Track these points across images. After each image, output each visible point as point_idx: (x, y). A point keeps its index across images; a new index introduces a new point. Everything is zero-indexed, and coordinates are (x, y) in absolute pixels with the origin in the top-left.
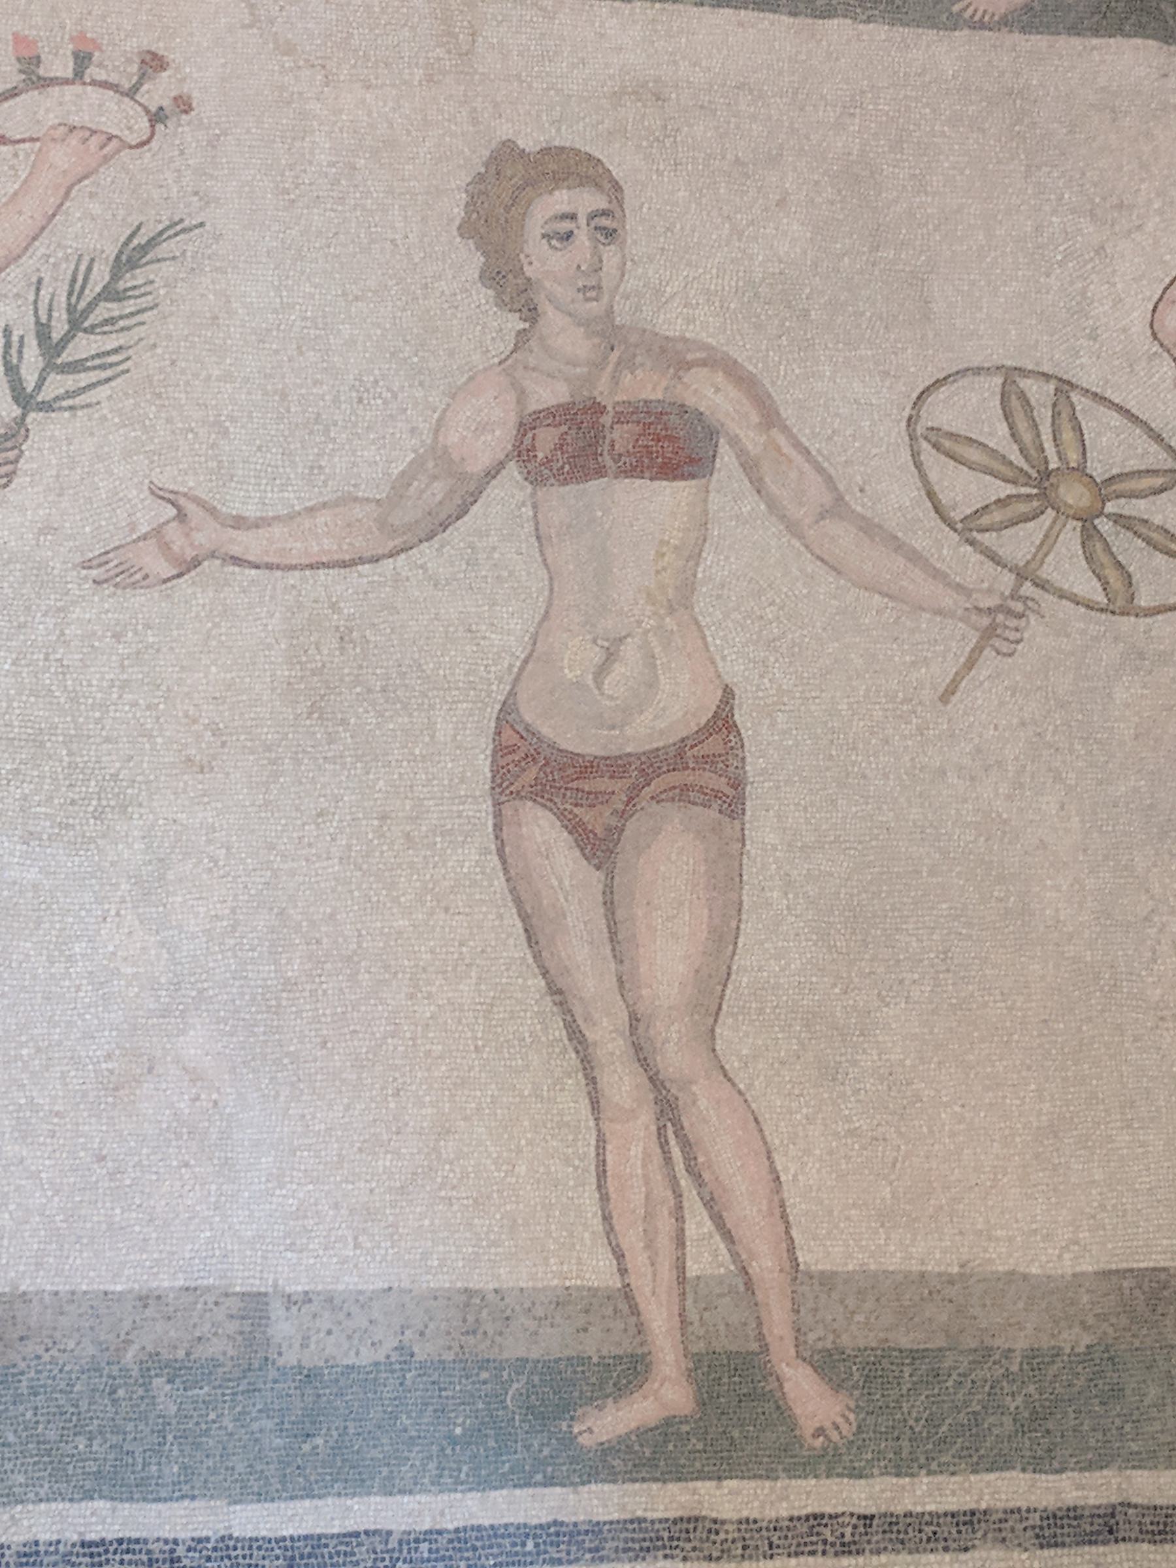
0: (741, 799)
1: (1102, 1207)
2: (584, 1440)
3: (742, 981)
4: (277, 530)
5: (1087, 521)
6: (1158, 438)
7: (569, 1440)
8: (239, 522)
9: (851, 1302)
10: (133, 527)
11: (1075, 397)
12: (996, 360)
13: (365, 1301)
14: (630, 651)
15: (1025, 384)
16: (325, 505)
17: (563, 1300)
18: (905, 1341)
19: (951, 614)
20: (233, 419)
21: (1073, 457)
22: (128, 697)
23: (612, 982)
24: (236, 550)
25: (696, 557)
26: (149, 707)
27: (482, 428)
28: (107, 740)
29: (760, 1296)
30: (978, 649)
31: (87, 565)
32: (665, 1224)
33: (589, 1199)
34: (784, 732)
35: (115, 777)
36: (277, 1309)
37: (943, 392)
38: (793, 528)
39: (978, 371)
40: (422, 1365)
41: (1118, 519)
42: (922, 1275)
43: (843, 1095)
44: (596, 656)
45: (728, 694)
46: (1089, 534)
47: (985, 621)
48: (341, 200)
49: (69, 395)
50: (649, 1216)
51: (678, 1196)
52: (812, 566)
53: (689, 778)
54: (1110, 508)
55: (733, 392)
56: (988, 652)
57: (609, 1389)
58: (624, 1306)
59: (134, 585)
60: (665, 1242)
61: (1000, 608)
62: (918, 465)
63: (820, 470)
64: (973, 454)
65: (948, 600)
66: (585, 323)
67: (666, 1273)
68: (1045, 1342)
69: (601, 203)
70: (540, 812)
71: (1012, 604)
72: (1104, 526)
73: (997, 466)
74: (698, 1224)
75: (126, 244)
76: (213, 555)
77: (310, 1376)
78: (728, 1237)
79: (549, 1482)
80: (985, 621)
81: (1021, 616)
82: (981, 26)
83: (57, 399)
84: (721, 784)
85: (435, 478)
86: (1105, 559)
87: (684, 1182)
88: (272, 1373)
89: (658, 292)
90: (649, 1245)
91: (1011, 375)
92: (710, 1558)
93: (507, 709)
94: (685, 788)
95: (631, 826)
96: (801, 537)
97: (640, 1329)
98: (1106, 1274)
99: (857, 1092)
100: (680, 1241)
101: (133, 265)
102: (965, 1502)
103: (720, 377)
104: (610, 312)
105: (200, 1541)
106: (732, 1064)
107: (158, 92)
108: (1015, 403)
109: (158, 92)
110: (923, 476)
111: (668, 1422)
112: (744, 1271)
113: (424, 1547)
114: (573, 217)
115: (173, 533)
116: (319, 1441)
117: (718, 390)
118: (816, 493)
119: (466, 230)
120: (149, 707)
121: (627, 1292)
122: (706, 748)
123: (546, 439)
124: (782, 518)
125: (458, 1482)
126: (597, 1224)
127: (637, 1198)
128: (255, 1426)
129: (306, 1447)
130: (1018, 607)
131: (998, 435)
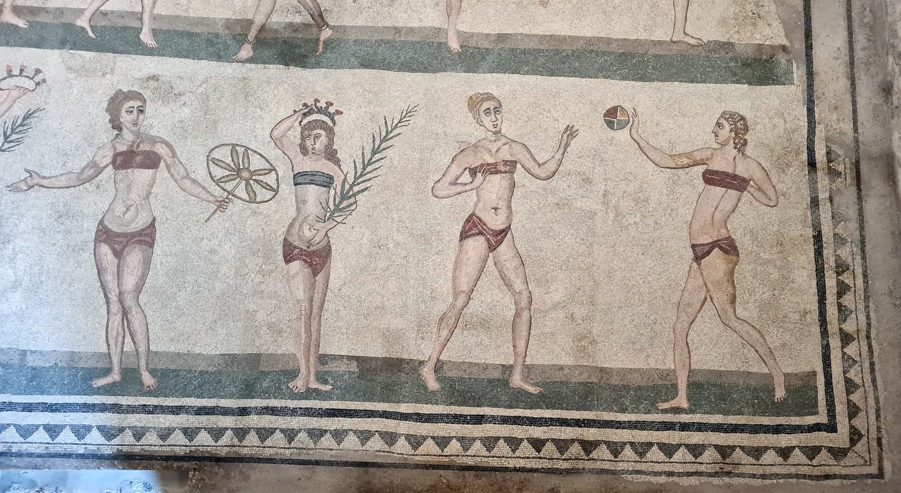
0: (154, 244)
1: (224, 339)
2: (94, 386)
3: (147, 285)
4: (53, 179)
5: (247, 181)
6: (268, 161)
7: (91, 386)
8: (44, 178)
9: (161, 358)
10: (20, 178)
11: (249, 151)
12: (231, 142)
13: (48, 353)
14: (133, 209)
15: (238, 149)
16: (65, 174)
17: (94, 354)
18: (172, 367)
19: (211, 202)
20: (46, 154)
21: (246, 166)
22: (14, 217)
23: (116, 284)
24: (42, 184)
25: (152, 187)
26: (18, 219)
27: (105, 156)
28: (7, 226)
29: (140, 356)
30: (216, 210)
31: (8, 187)
32: (120, 339)
33: (103, 333)
34: (166, 228)
35: (8, 235)
36: (28, 353)
37: (217, 150)
38: (176, 181)
39: (226, 145)
40: (60, 368)
41: (255, 180)
42: (178, 353)
43: (166, 312)
44: (124, 209)
45: (154, 219)
46: (247, 184)
47: (219, 204)
48: (78, 103)
49: (9, 148)
50: (117, 338)
51: (124, 333)
52: (179, 190)
53: (142, 238)
54: (254, 178)
55: (166, 149)
56: (218, 211)
57: (102, 375)
58: (108, 357)
59: (18, 192)
60: (119, 343)
61: (223, 201)
62: (208, 167)
63: (183, 166)
64: (223, 165)
65: (211, 199)
66: (132, 132)
67: (119, 349)
68: (205, 369)
69: (139, 103)
70: (105, 245)
71: (226, 200)
72: (251, 182)
73: (226, 167)
74: (128, 339)
75: (27, 112)
76: (37, 185)
77: (34, 369)
78: (134, 343)
79: (85, 394)
80: (219, 204)
81: (227, 203)
82: (240, 62)
83: (6, 149)
84: (149, 240)
85: (92, 168)
86: (250, 190)
87: (126, 330)
88: (26, 368)
89: (151, 125)
90: (116, 344)
91: (234, 146)
92: (119, 413)
93: (101, 222)
94: (141, 241)
95: (126, 250)
96: (177, 183)
97: (111, 362)
98: (222, 355)
99: (170, 311)
100: (123, 343)
101: (27, 118)
102: (180, 404)
103: (164, 145)
104: (139, 129)
105: (4, 402)
106: (142, 304)
107: (38, 78)
108: (234, 152)
109: (38, 78)
110: (209, 169)
111: (114, 382)
112: (137, 350)
113: (54, 407)
114: (133, 107)
115: (29, 180)
116: (34, 383)
117: (162, 148)
118: (182, 172)
119: (107, 110)
120: (18, 219)
121: (109, 354)
122: (147, 232)
123: (119, 159)
124: (174, 179)
125: (64, 393)
126: (104, 338)
127: (115, 333)
128: (20, 379)
129: (31, 384)
130: (227, 201)
131: (229, 160)
